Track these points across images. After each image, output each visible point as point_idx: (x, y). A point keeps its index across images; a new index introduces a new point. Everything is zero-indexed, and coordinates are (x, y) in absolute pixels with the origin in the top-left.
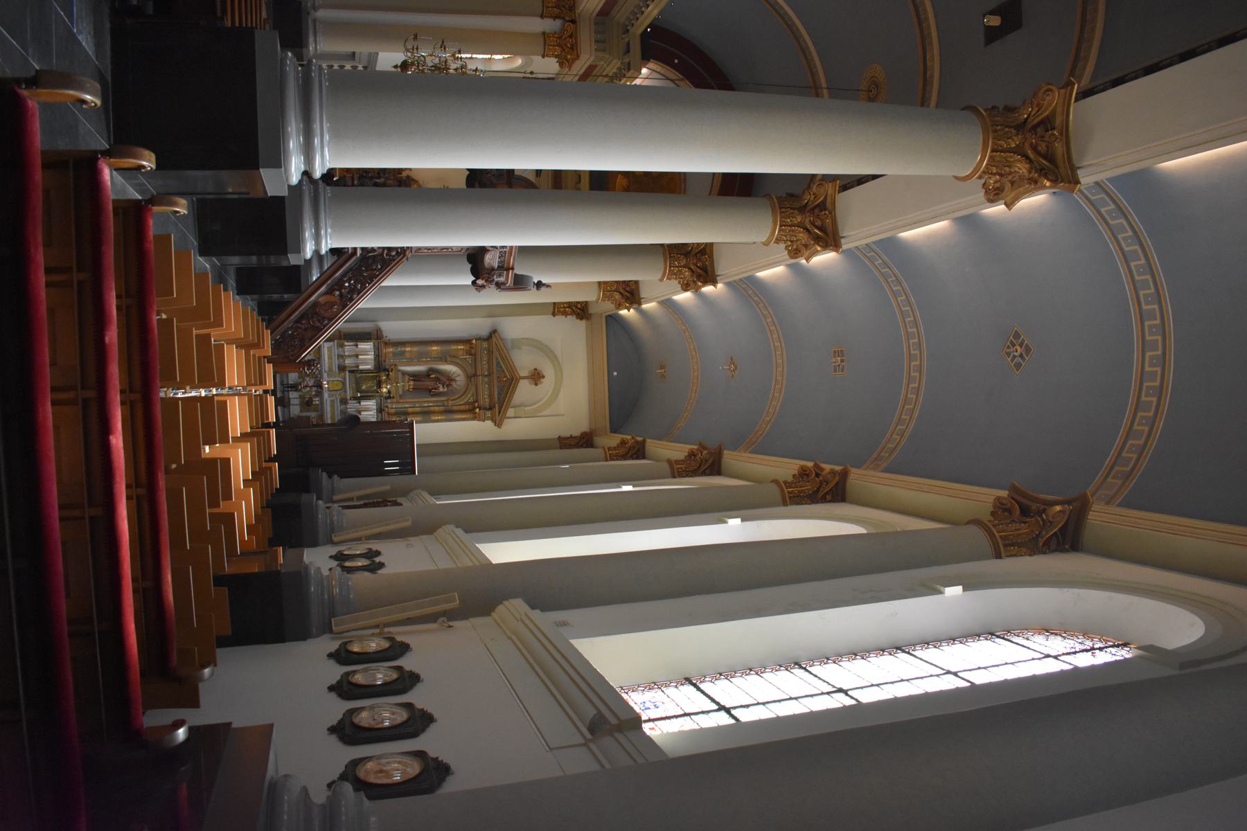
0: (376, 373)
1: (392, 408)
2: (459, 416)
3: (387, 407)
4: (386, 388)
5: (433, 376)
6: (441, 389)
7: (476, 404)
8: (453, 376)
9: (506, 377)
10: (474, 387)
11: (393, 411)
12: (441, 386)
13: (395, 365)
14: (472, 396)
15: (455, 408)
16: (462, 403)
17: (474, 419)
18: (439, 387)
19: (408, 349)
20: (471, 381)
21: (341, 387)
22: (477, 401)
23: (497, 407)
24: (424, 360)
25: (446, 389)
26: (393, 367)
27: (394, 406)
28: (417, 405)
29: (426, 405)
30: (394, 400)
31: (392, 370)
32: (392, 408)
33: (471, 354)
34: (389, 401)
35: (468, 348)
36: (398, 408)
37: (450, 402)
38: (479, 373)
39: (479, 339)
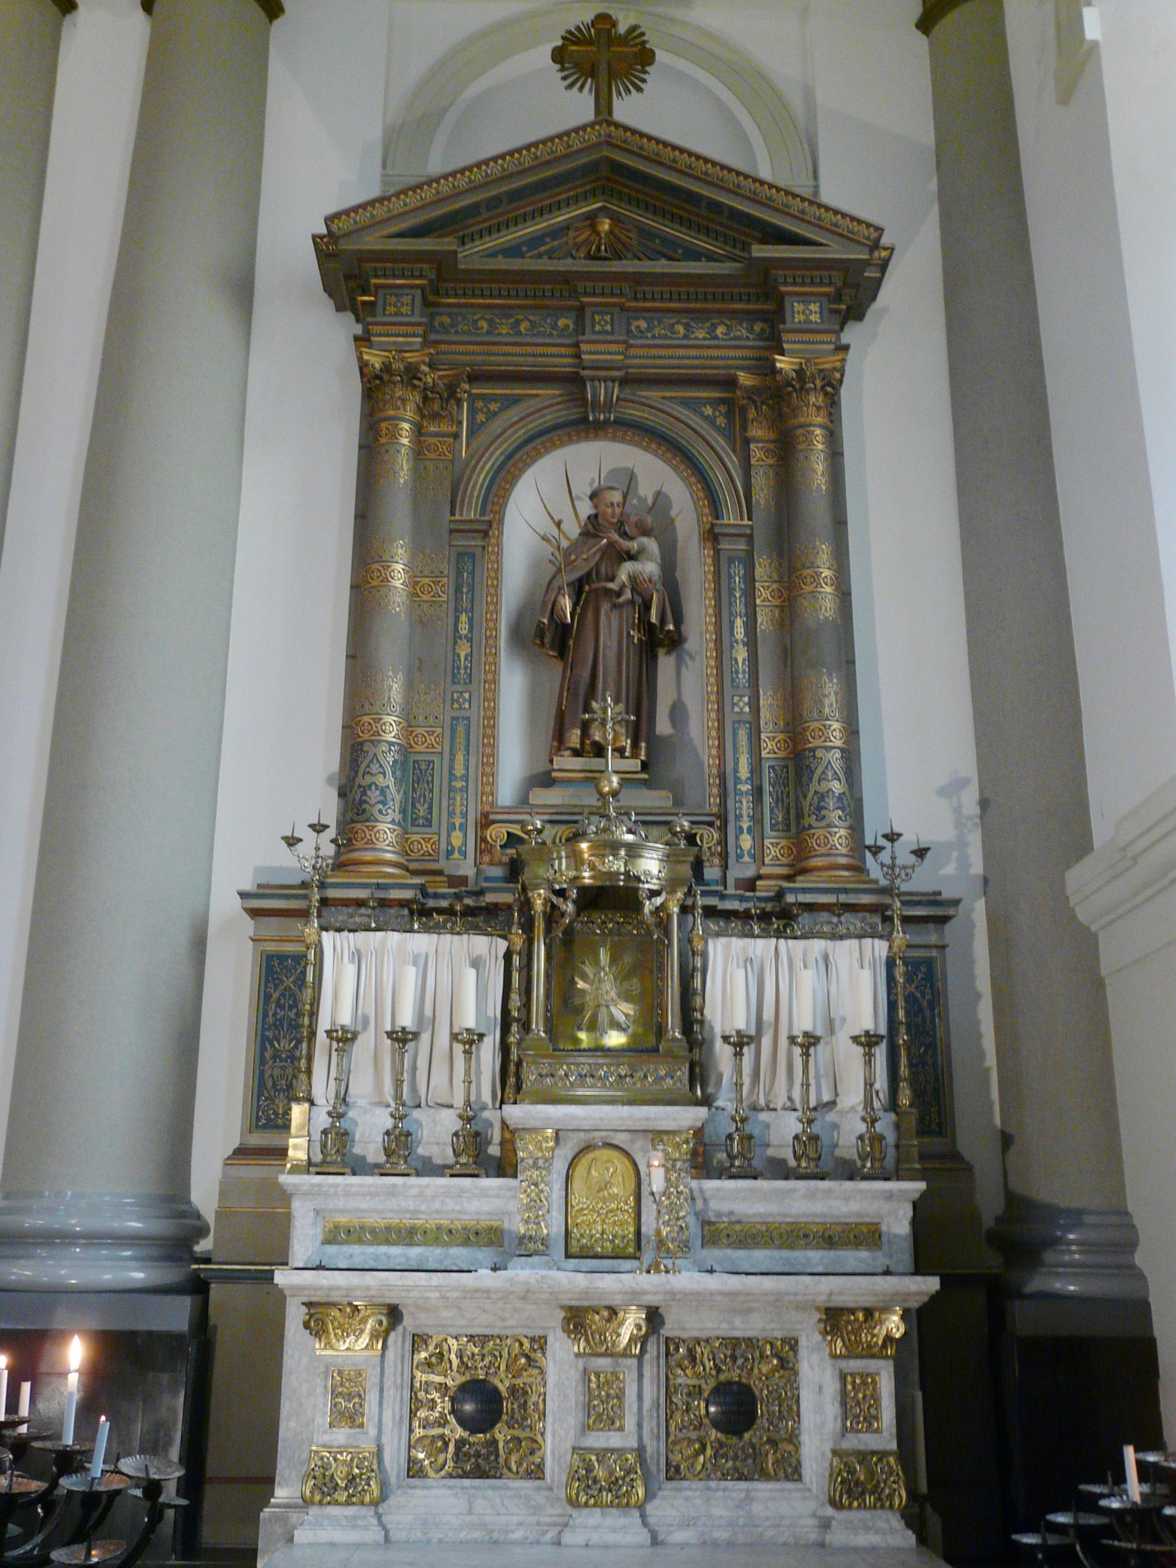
0: (528, 927)
1: (758, 855)
2: (819, 467)
3: (750, 884)
4: (633, 851)
5: (567, 603)
6: (649, 568)
7: (745, 379)
8: (564, 511)
9: (591, 219)
10: (653, 395)
11: (775, 847)
12: (625, 571)
13: (485, 822)
14: (685, 402)
15: (762, 494)
16: (733, 462)
17: (831, 386)
18: (633, 579)
19: (391, 729)
20: (609, 405)
21: (619, 1164)
22: (730, 383)
23: (759, 251)
24: (464, 629)
25: (652, 545)
26: (497, 833)
27: (746, 842)
28: (743, 705)
29: (741, 654)
30: (709, 838)
31: (512, 840)
32: (758, 855)
33: (451, 392)
34: (711, 872)
35: (415, 397)
36: (758, 820)
37: (730, 518)
38: (563, 363)
39: (363, 340)
